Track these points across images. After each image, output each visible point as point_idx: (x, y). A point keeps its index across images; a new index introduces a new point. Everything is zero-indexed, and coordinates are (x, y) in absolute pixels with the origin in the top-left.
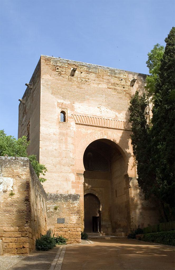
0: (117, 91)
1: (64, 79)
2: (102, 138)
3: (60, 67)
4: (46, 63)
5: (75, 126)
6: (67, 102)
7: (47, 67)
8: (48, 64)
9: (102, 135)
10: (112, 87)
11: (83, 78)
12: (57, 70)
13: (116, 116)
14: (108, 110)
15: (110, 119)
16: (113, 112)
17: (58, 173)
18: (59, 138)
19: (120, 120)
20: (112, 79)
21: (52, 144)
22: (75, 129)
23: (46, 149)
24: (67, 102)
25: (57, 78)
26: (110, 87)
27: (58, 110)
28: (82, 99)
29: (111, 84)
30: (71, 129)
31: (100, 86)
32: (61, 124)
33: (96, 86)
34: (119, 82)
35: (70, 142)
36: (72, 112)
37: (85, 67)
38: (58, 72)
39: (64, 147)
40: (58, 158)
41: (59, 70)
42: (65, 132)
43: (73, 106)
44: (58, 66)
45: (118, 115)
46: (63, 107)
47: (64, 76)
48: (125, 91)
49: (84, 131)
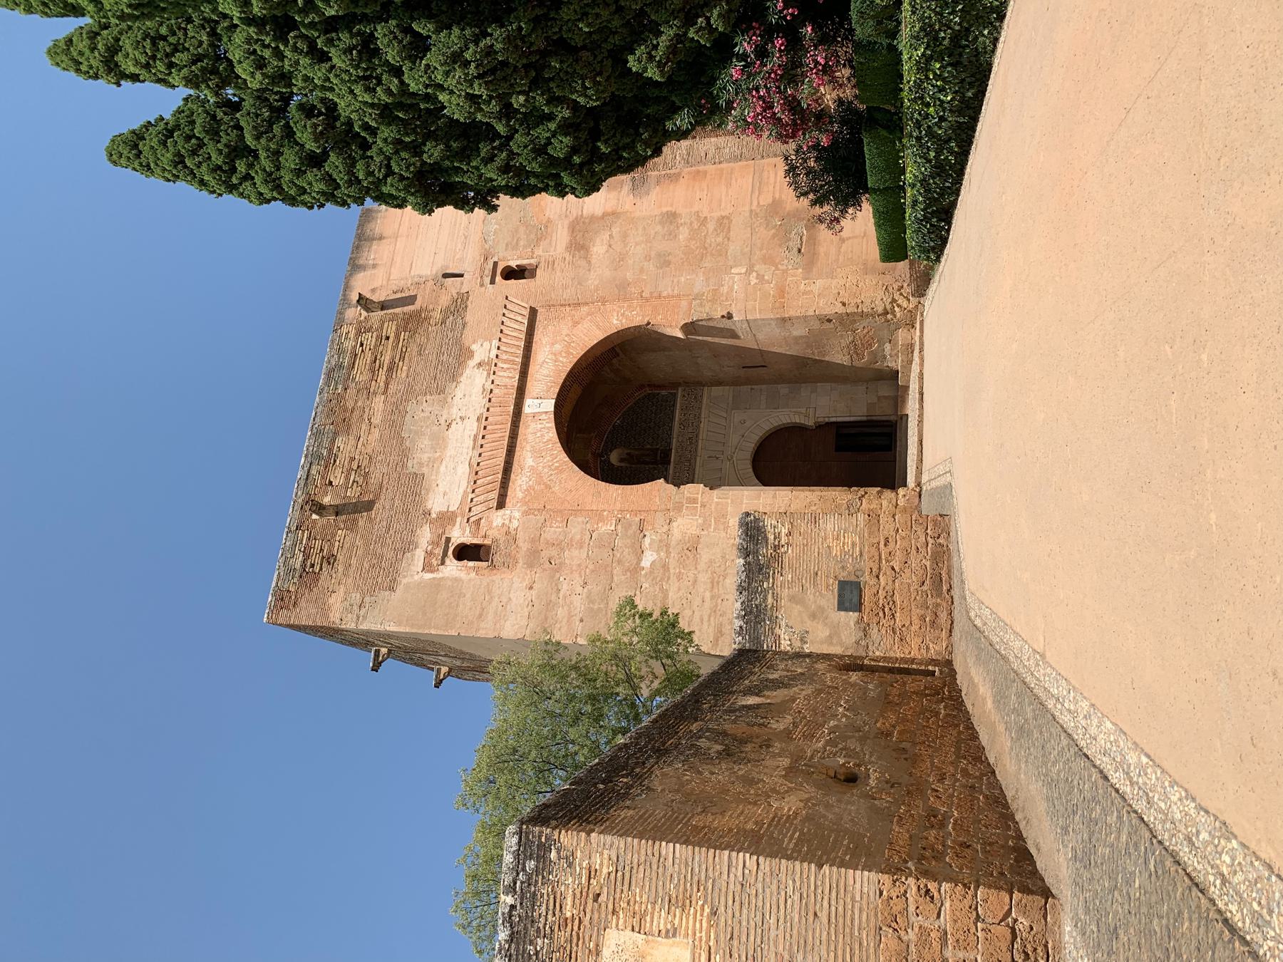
0: (397, 362)
1: (346, 546)
2: (552, 416)
3: (307, 556)
4: (291, 607)
5: (508, 512)
6: (425, 535)
7: (303, 603)
8: (293, 597)
9: (540, 418)
10: (384, 377)
11: (347, 478)
12: (317, 569)
13: (480, 364)
14: (459, 393)
15: (489, 386)
16: (465, 375)
17: (669, 578)
18: (544, 570)
19: (494, 352)
20: (357, 379)
21: (565, 597)
22: (517, 515)
23: (581, 621)
24: (425, 535)
25: (341, 570)
26: (382, 384)
27: (448, 568)
28: (415, 485)
29: (374, 382)
30: (515, 524)
31: (376, 420)
32: (498, 559)
33: (376, 433)
34: (369, 356)
35: (560, 530)
36: (459, 519)
37: (313, 472)
38: (321, 565)
39: (575, 553)
40: (615, 578)
41: (318, 560)
42: (524, 546)
45: (477, 359)
46: (439, 551)
47: (337, 543)
48: (397, 336)
49: (524, 479)
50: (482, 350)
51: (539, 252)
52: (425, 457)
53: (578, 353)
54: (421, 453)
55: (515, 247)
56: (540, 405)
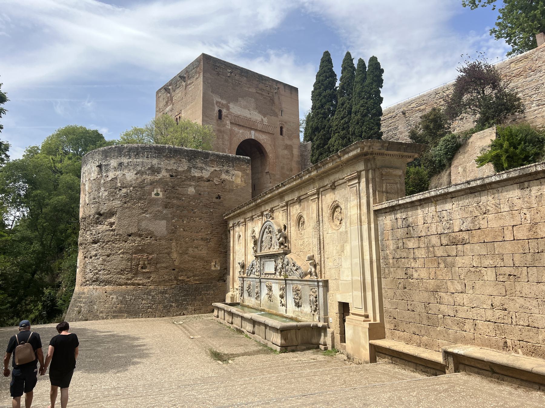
3: (219, 67)
11: (237, 80)
12: (216, 70)
13: (262, 119)
14: (256, 113)
19: (265, 123)
28: (235, 99)
37: (239, 70)
43: (229, 107)
44: (216, 66)
45: (263, 119)
50: (265, 120)
51: (286, 137)
52: (242, 103)
53: (264, 145)
54: (243, 102)
55: (287, 130)
56: (253, 135)
